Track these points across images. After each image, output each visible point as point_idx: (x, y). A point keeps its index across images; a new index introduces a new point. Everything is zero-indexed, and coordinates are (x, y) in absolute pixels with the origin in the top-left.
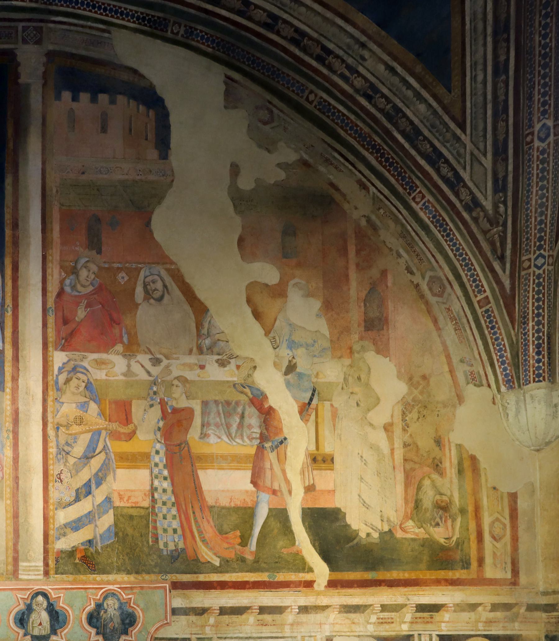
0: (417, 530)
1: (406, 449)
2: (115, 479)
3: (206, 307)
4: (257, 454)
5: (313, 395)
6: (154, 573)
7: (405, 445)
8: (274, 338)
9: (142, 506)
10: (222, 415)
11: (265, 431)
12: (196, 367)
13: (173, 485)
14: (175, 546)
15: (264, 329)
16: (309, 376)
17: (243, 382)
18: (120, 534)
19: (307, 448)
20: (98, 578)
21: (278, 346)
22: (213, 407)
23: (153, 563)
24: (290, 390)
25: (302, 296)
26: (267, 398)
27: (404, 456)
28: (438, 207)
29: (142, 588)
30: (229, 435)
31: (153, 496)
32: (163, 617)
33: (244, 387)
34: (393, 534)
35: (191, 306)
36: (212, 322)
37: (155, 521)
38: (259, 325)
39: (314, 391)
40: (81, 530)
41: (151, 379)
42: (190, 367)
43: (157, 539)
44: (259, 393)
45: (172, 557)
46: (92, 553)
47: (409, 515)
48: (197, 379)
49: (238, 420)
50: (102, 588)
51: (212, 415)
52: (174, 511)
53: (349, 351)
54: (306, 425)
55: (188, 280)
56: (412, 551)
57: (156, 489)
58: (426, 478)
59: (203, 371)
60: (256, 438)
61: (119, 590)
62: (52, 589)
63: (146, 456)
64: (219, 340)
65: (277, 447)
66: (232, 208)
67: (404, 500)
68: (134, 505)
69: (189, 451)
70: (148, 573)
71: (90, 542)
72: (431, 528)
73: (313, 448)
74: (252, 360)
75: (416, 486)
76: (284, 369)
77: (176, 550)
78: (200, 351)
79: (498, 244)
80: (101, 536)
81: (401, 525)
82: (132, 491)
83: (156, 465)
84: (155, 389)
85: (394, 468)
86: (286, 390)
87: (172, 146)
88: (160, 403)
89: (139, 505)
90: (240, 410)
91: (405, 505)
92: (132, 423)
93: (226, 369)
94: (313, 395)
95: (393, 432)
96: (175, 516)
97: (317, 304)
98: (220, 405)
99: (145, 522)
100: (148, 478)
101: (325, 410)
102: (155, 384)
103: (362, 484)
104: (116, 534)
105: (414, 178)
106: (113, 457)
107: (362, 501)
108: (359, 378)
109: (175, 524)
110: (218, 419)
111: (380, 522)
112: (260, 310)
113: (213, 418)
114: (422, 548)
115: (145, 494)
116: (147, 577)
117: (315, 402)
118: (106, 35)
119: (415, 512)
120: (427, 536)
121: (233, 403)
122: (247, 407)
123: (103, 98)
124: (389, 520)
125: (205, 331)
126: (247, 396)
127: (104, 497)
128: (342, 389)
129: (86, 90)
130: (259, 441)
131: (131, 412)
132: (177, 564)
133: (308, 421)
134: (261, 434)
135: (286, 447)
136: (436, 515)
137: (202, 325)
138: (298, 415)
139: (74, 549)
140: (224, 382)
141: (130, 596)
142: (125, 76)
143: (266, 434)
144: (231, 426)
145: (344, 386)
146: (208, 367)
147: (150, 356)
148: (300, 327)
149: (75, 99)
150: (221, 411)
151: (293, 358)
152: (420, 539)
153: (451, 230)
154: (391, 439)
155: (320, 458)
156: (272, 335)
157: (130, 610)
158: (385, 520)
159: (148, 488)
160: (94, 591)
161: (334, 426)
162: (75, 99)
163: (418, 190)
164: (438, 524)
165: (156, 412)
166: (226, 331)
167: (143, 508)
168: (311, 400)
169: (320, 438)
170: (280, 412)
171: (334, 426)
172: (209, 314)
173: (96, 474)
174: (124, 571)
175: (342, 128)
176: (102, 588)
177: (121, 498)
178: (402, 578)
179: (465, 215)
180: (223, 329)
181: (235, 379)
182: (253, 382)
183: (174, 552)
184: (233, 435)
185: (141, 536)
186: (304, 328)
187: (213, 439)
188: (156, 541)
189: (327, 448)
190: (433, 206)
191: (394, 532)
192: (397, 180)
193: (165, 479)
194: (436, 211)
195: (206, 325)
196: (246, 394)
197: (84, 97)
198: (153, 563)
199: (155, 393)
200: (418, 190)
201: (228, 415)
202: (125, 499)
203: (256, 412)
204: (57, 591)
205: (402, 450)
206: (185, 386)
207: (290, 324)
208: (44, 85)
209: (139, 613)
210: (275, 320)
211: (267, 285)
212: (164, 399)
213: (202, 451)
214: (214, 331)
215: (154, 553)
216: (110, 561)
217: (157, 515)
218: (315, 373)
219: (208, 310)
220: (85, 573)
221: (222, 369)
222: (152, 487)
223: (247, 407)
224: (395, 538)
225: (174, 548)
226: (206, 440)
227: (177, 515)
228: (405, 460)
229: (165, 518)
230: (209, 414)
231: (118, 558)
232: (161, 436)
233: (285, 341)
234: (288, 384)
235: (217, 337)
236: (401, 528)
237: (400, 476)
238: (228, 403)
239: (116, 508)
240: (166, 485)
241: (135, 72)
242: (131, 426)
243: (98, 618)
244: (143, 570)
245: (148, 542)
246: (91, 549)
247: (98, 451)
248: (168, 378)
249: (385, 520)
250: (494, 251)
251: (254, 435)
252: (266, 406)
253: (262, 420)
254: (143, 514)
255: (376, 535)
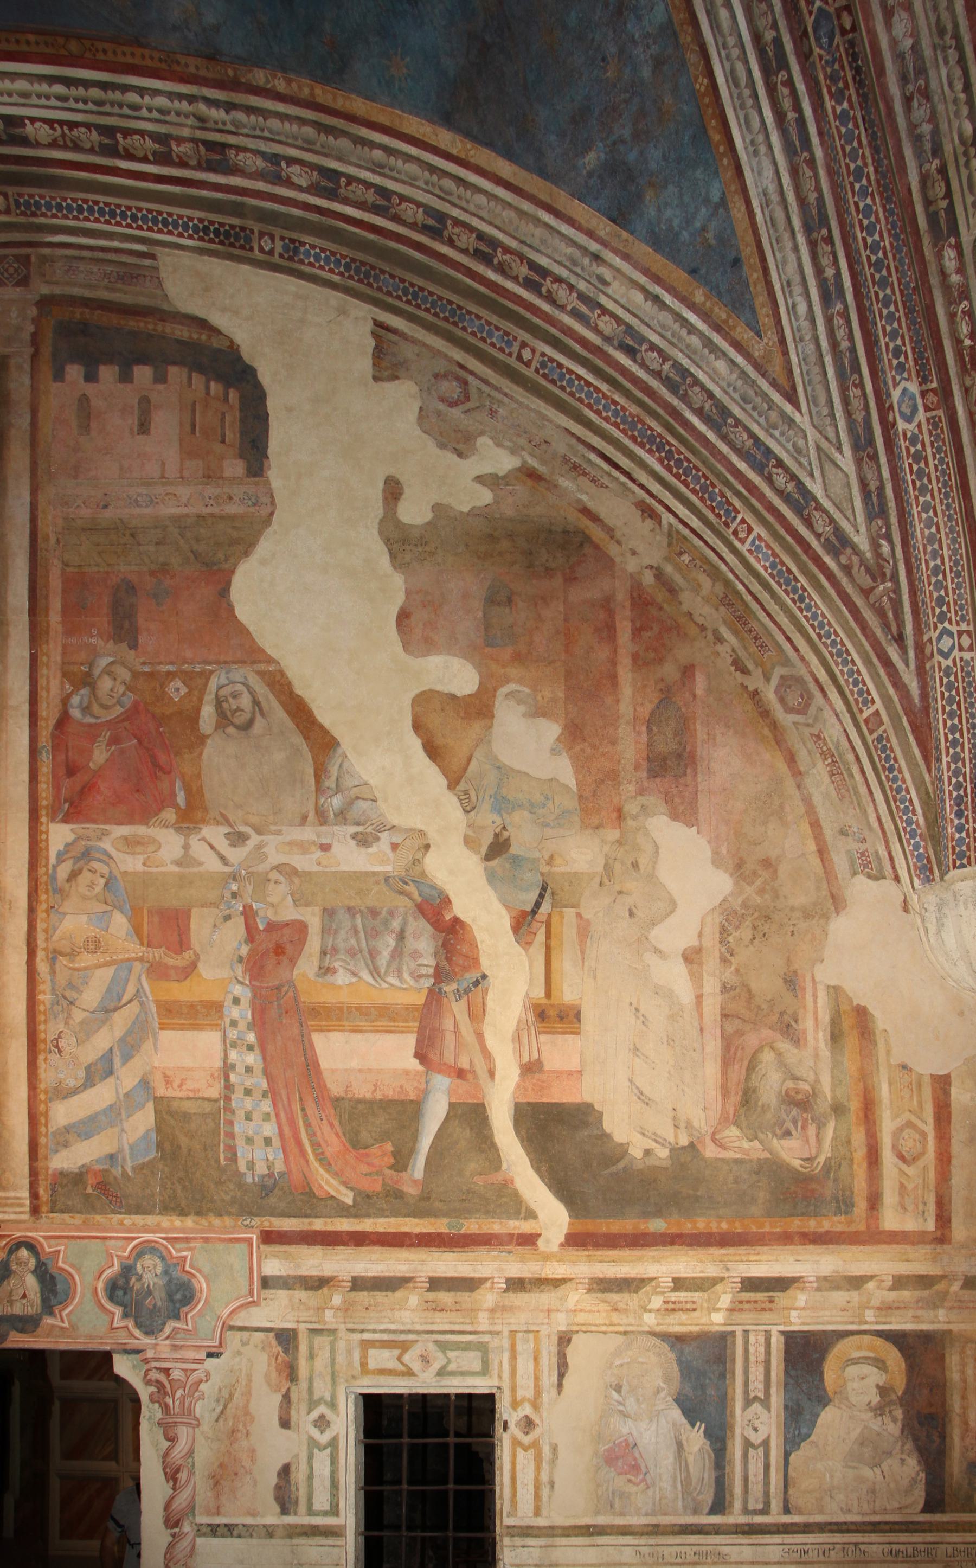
0: (746, 1145)
1: (727, 995)
2: (156, 1049)
3: (334, 739)
4: (427, 1003)
5: (541, 896)
6: (230, 1214)
7: (725, 989)
8: (466, 792)
9: (206, 1095)
10: (362, 934)
11: (444, 963)
12: (313, 848)
13: (264, 1059)
14: (269, 1168)
15: (446, 777)
16: (535, 861)
17: (403, 873)
18: (167, 1145)
19: (527, 994)
20: (128, 1220)
21: (474, 808)
22: (342, 916)
23: (228, 1198)
24: (495, 889)
25: (524, 715)
26: (450, 902)
27: (722, 1009)
28: (778, 549)
29: (206, 1240)
30: (375, 971)
31: (227, 1077)
32: (245, 1290)
33: (406, 883)
34: (698, 1151)
35: (306, 738)
36: (345, 765)
37: (231, 1123)
38: (437, 769)
39: (544, 888)
40: (96, 1137)
41: (227, 869)
42: (303, 848)
43: (235, 1154)
44: (435, 893)
45: (263, 1187)
46: (115, 1178)
47: (731, 1116)
48: (316, 868)
49: (392, 943)
50: (134, 1239)
51: (342, 934)
52: (267, 1106)
53: (615, 815)
54: (526, 951)
55: (299, 691)
56: (736, 1181)
57: (233, 1067)
58: (766, 1050)
59: (328, 854)
60: (427, 976)
61: (164, 1242)
62: (45, 1238)
63: (215, 1008)
64: (358, 798)
65: (467, 991)
66: (385, 560)
67: (719, 1091)
68: (191, 1095)
69: (296, 999)
70: (219, 1215)
71: (112, 1157)
72: (775, 1140)
73: (539, 993)
74: (422, 833)
75: (746, 1063)
76: (484, 850)
77: (271, 1175)
78: (322, 818)
79: (890, 615)
80: (131, 1148)
81: (714, 1134)
82: (189, 1070)
83: (234, 1023)
84: (234, 887)
85: (702, 1030)
86: (488, 888)
87: (270, 452)
88: (244, 913)
89: (200, 1095)
90: (396, 924)
91: (723, 1099)
92: (189, 948)
93: (370, 850)
94: (541, 896)
95: (701, 964)
96: (268, 1114)
97: (552, 730)
98: (358, 916)
99: (212, 1125)
100: (219, 1047)
101: (567, 924)
102: (235, 879)
103: (637, 1060)
104: (160, 1146)
105: (729, 494)
106: (154, 1009)
107: (636, 1091)
108: (635, 865)
109: (269, 1129)
110: (353, 942)
111: (672, 1130)
112: (439, 741)
113: (343, 939)
114: (755, 1177)
115: (212, 1075)
116: (217, 1222)
117: (545, 908)
118: (147, 262)
119: (742, 1111)
120: (766, 1155)
121: (384, 912)
122: (411, 919)
123: (143, 373)
124: (689, 1126)
125: (330, 783)
126: (411, 898)
127: (137, 1080)
128: (601, 884)
129: (109, 361)
130: (432, 981)
131: (189, 929)
132: (272, 1200)
133: (529, 943)
134: (437, 968)
135: (486, 991)
136: (784, 1116)
137: (326, 771)
138: (511, 933)
139: (84, 1170)
140: (367, 874)
141: (184, 1254)
142: (182, 332)
143: (447, 967)
144: (379, 953)
145: (606, 880)
146: (336, 848)
147: (226, 829)
148: (519, 772)
149: (91, 377)
150: (360, 927)
151: (504, 828)
152: (751, 1161)
153: (804, 590)
154: (696, 978)
155: (552, 1013)
156: (462, 786)
157: (185, 1277)
158: (683, 1125)
159: (218, 1064)
160: (120, 1243)
161: (583, 953)
162: (91, 377)
163: (739, 517)
164: (788, 1133)
165: (237, 928)
166: (371, 782)
167: (209, 1100)
168: (538, 905)
169: (555, 976)
170: (474, 928)
171: (583, 953)
172: (339, 751)
173: (122, 1040)
174: (173, 1209)
175: (589, 406)
176: (134, 1239)
177: (168, 1081)
178: (715, 1230)
179: (827, 559)
180: (365, 778)
181: (389, 868)
182: (423, 874)
183: (266, 1179)
184: (383, 971)
185: (205, 1150)
186: (527, 774)
187: (342, 978)
188: (233, 1158)
189: (568, 994)
190: (768, 546)
191: (699, 1146)
192: (702, 499)
193: (250, 1048)
194: (775, 555)
195: (334, 771)
196: (409, 896)
197: (107, 373)
198: (228, 1198)
199: (234, 895)
200: (739, 517)
201: (373, 934)
202: (175, 1085)
203: (429, 927)
204: (53, 1242)
205: (719, 998)
206: (292, 882)
207: (499, 768)
208: (35, 356)
209: (201, 1283)
210: (469, 760)
211: (453, 697)
212: (251, 907)
213: (322, 1000)
214: (348, 782)
215: (230, 1181)
216: (148, 1191)
217: (233, 1112)
218: (547, 857)
219: (338, 744)
220: (103, 1212)
221: (363, 850)
222: (225, 1063)
223: (411, 919)
224: (704, 1159)
225: (267, 1172)
226: (329, 978)
227: (273, 1114)
228: (725, 1016)
229: (248, 1117)
230: (336, 932)
231: (164, 1186)
232: (244, 972)
233: (487, 798)
234: (491, 877)
235: (354, 792)
236: (714, 1140)
237: (714, 1046)
238: (374, 913)
239: (158, 1100)
240: (252, 1059)
241: (203, 324)
242: (188, 955)
243: (126, 1289)
244: (209, 1210)
245: (218, 1161)
246: (114, 1171)
247: (124, 1001)
248: (261, 868)
249: (683, 1125)
250: (886, 625)
251: (423, 971)
252: (448, 917)
253: (440, 943)
254: (207, 1110)
255: (663, 1153)
